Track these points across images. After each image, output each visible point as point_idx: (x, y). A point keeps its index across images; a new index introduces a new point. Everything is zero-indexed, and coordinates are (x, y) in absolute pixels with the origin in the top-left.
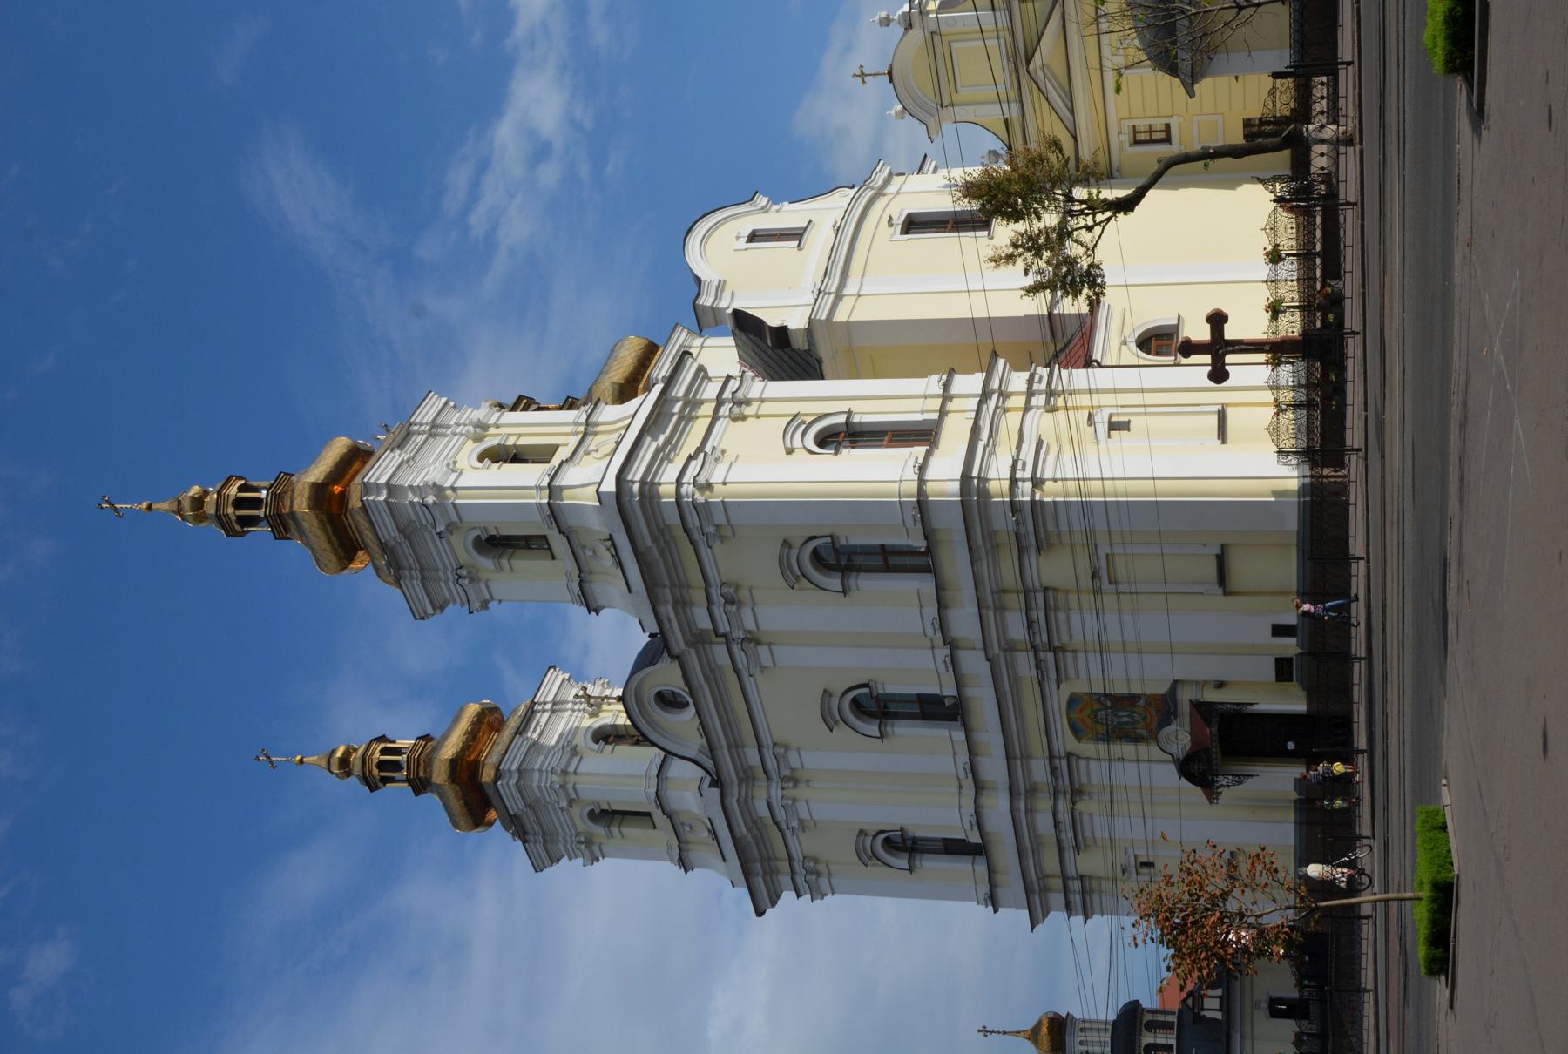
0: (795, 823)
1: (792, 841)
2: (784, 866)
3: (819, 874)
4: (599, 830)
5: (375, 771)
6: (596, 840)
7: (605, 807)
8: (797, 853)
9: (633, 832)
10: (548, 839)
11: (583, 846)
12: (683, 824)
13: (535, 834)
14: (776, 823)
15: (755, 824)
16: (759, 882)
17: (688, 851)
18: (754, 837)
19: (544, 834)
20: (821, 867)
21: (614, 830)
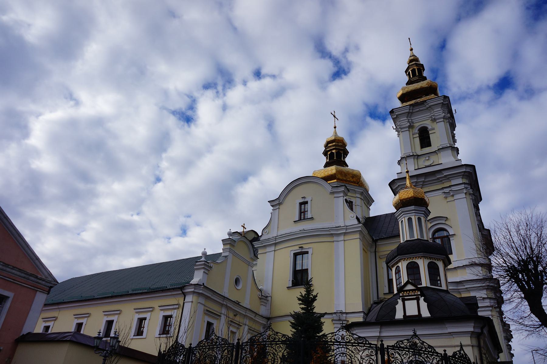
4: (416, 131)
5: (418, 68)
6: (411, 130)
7: (430, 132)
9: (417, 141)
10: (409, 114)
12: (429, 157)
14: (450, 186)
15: (448, 178)
18: (438, 179)
19: (412, 113)
21: (417, 135)
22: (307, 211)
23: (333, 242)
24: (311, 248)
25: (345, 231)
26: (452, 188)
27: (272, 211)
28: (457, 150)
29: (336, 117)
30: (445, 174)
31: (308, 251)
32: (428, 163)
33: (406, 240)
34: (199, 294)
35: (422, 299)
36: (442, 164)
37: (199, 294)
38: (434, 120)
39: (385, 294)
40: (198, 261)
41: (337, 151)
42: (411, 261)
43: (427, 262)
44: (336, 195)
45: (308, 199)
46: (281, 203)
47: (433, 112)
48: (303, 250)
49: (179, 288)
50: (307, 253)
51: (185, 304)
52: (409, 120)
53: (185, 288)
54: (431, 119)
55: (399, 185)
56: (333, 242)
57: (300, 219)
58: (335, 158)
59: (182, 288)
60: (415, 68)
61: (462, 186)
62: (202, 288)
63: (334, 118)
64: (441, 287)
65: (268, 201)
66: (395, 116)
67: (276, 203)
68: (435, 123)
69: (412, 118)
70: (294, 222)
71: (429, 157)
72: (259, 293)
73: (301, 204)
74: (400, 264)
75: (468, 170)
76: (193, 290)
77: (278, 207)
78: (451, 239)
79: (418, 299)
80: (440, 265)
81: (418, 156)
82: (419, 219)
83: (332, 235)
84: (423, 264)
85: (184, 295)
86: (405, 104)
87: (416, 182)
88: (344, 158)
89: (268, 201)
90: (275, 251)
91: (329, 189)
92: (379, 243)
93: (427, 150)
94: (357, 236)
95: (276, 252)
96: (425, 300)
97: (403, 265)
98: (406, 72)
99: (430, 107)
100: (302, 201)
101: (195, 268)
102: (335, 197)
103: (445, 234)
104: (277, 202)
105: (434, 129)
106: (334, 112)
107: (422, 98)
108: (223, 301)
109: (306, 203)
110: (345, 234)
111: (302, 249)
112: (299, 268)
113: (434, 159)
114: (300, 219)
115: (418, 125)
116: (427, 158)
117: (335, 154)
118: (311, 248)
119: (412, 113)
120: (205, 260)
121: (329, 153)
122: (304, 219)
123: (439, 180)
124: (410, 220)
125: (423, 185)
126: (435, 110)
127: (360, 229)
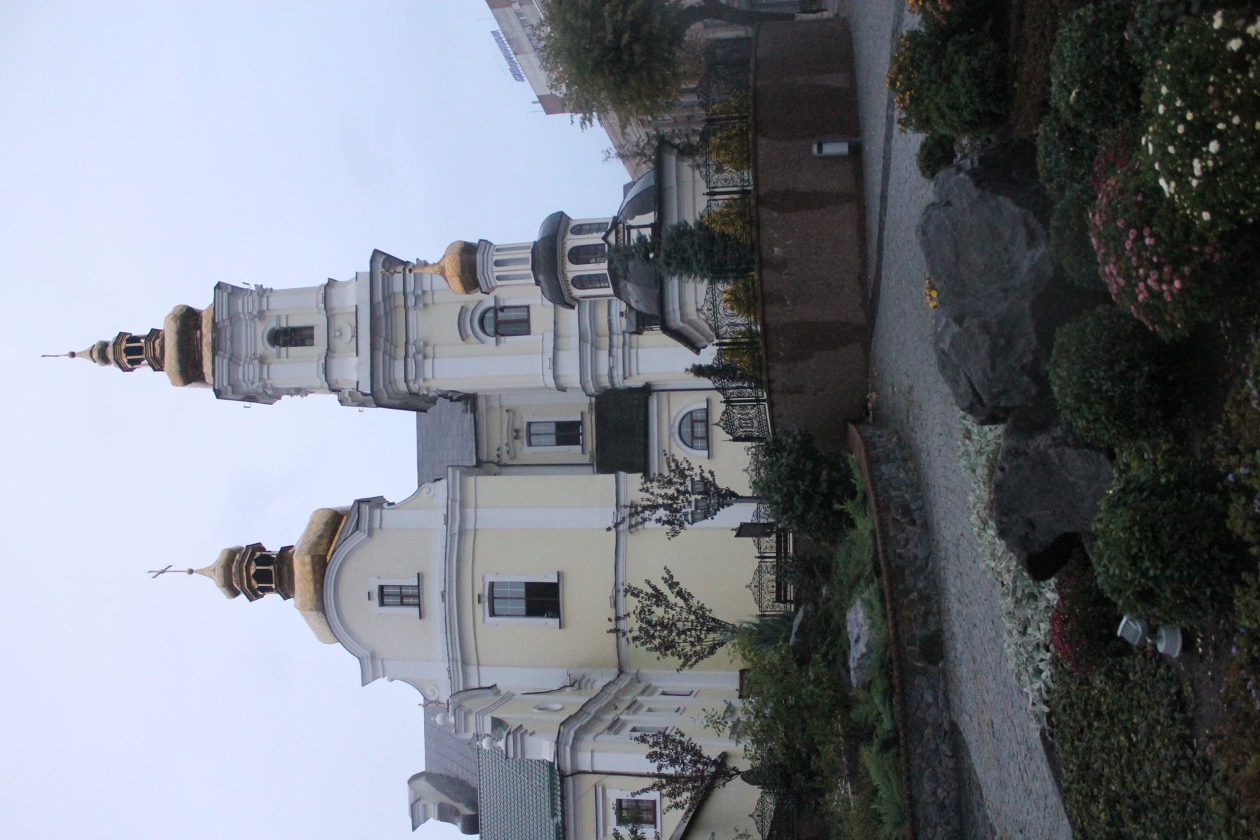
0: (420, 293)
1: (412, 314)
2: (401, 352)
3: (425, 357)
4: (273, 351)
5: (125, 342)
6: (268, 361)
7: (284, 325)
9: (294, 351)
13: (226, 352)
15: (388, 296)
16: (380, 355)
17: (332, 358)
18: (386, 314)
20: (429, 350)
21: (284, 349)
22: (401, 587)
23: (475, 530)
24: (483, 576)
25: (457, 505)
26: (408, 291)
27: (386, 678)
28: (331, 283)
29: (163, 568)
30: (380, 299)
31: (490, 583)
32: (348, 332)
33: (531, 272)
34: (576, 739)
35: (631, 222)
36: (356, 306)
37: (576, 739)
38: (261, 315)
39: (583, 452)
40: (505, 752)
41: (253, 563)
42: (567, 258)
43: (570, 236)
44: (376, 524)
46: (371, 653)
47: (244, 313)
48: (486, 594)
49: (562, 781)
50: (492, 585)
51: (595, 769)
53: (562, 768)
54: (257, 319)
55: (384, 386)
56: (475, 530)
57: (419, 605)
58: (271, 568)
59: (563, 776)
60: (123, 348)
62: (566, 730)
63: (166, 573)
64: (608, 223)
65: (363, 685)
66: (230, 388)
67: (372, 667)
68: (268, 314)
69: (244, 353)
70: (420, 617)
72: (568, 690)
73: (382, 604)
74: (570, 276)
75: (381, 259)
76: (568, 749)
77: (379, 663)
78: (502, 304)
79: (630, 227)
81: (328, 349)
83: (462, 532)
85: (577, 773)
86: (207, 368)
87: (385, 353)
89: (363, 685)
90: (479, 665)
91: (360, 536)
92: (484, 458)
93: (320, 335)
95: (481, 662)
96: (632, 218)
97: (573, 270)
98: (125, 369)
99: (230, 318)
101: (519, 757)
102: (380, 527)
103: (490, 315)
104: (368, 663)
105: (279, 317)
106: (150, 572)
108: (589, 714)
109: (381, 588)
110: (463, 505)
111: (484, 596)
112: (521, 606)
113: (344, 324)
114: (419, 605)
115: (263, 347)
116: (338, 334)
117: (260, 568)
118: (483, 576)
119: (232, 355)
120: (504, 740)
121: (254, 582)
122: (418, 596)
123: (390, 312)
124: (498, 263)
125: (392, 344)
126: (240, 310)
127: (458, 472)
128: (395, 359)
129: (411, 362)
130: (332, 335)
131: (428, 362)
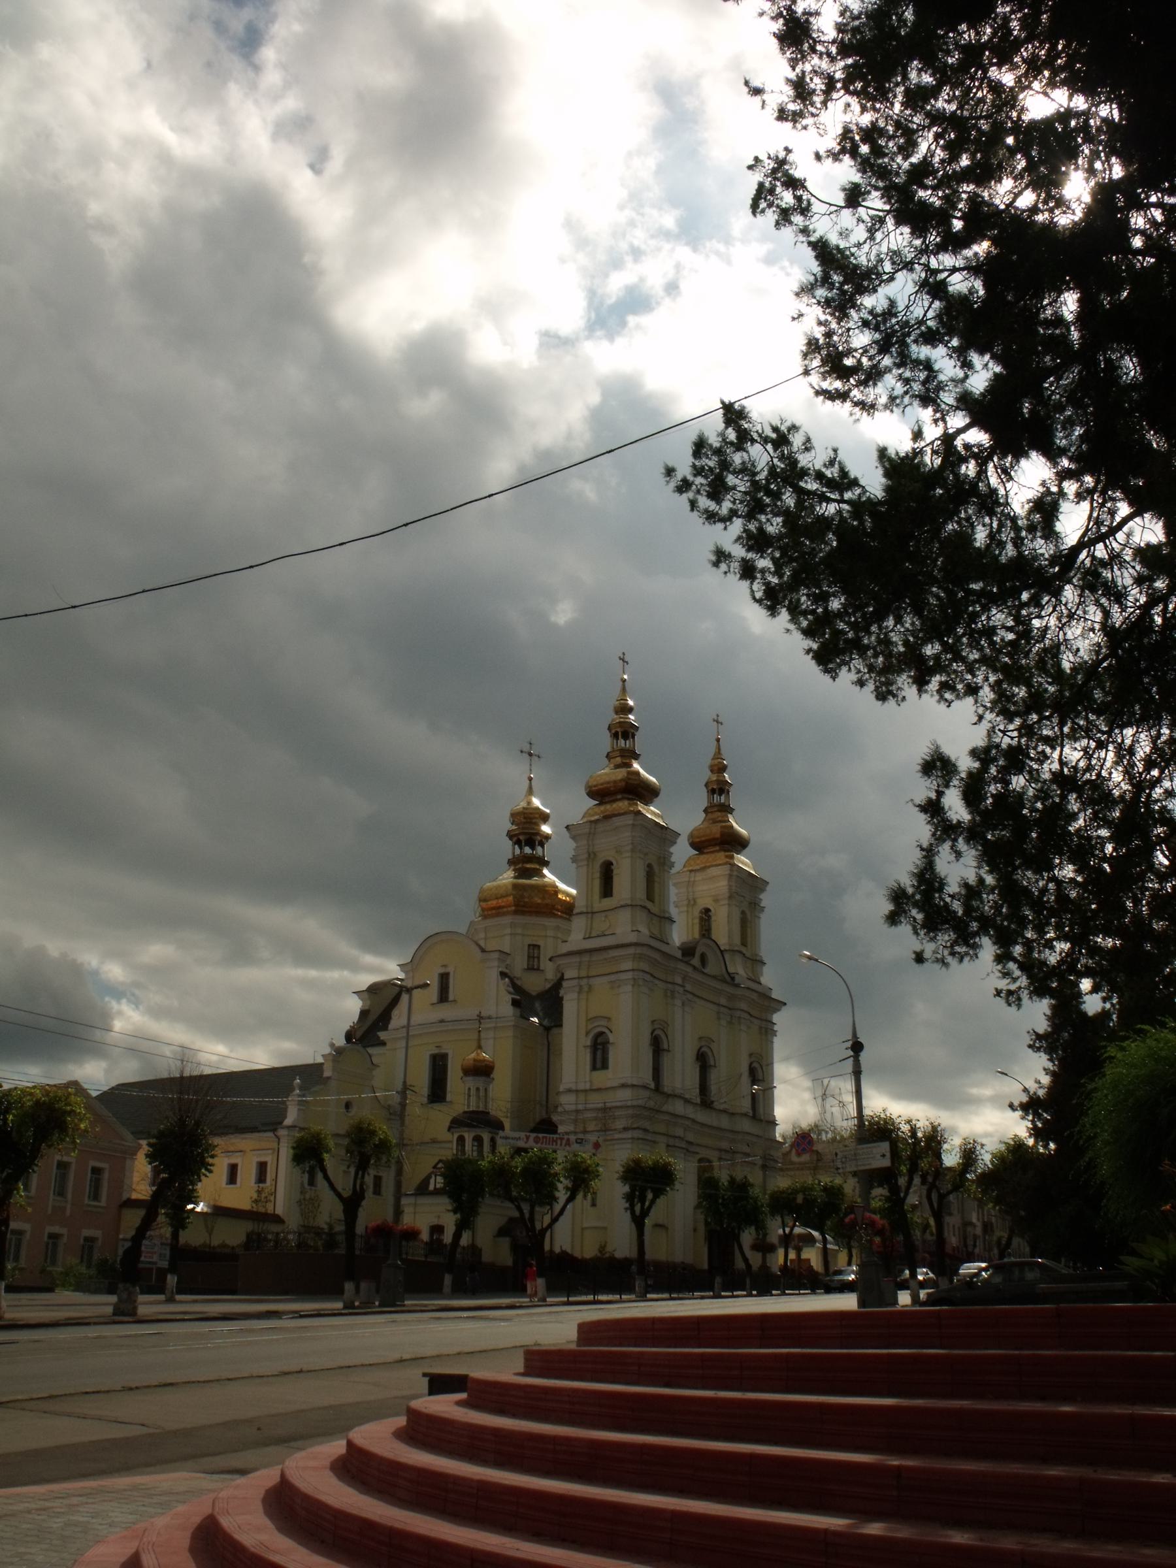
2: (583, 973)
3: (580, 992)
7: (615, 872)
8: (592, 981)
11: (586, 856)
12: (606, 916)
14: (617, 972)
16: (576, 959)
19: (594, 834)
21: (597, 875)
25: (493, 1025)
26: (619, 974)
41: (528, 836)
45: (450, 969)
52: (589, 845)
59: (274, 1130)
61: (630, 975)
71: (606, 916)
80: (486, 1137)
81: (593, 913)
82: (478, 1089)
84: (469, 1136)
88: (542, 845)
94: (510, 1033)
100: (442, 970)
107: (615, 805)
121: (515, 839)
127: (513, 1023)
128: (579, 969)
129: (575, 982)
130: (603, 914)
131: (575, 995)
